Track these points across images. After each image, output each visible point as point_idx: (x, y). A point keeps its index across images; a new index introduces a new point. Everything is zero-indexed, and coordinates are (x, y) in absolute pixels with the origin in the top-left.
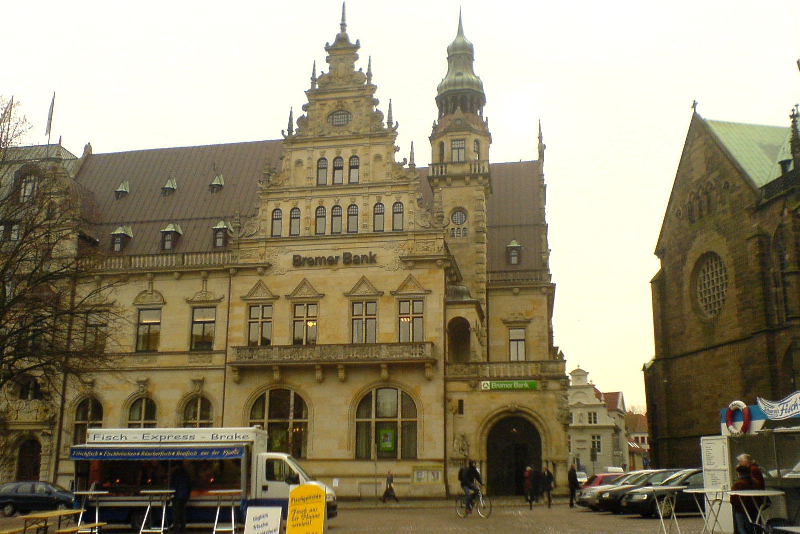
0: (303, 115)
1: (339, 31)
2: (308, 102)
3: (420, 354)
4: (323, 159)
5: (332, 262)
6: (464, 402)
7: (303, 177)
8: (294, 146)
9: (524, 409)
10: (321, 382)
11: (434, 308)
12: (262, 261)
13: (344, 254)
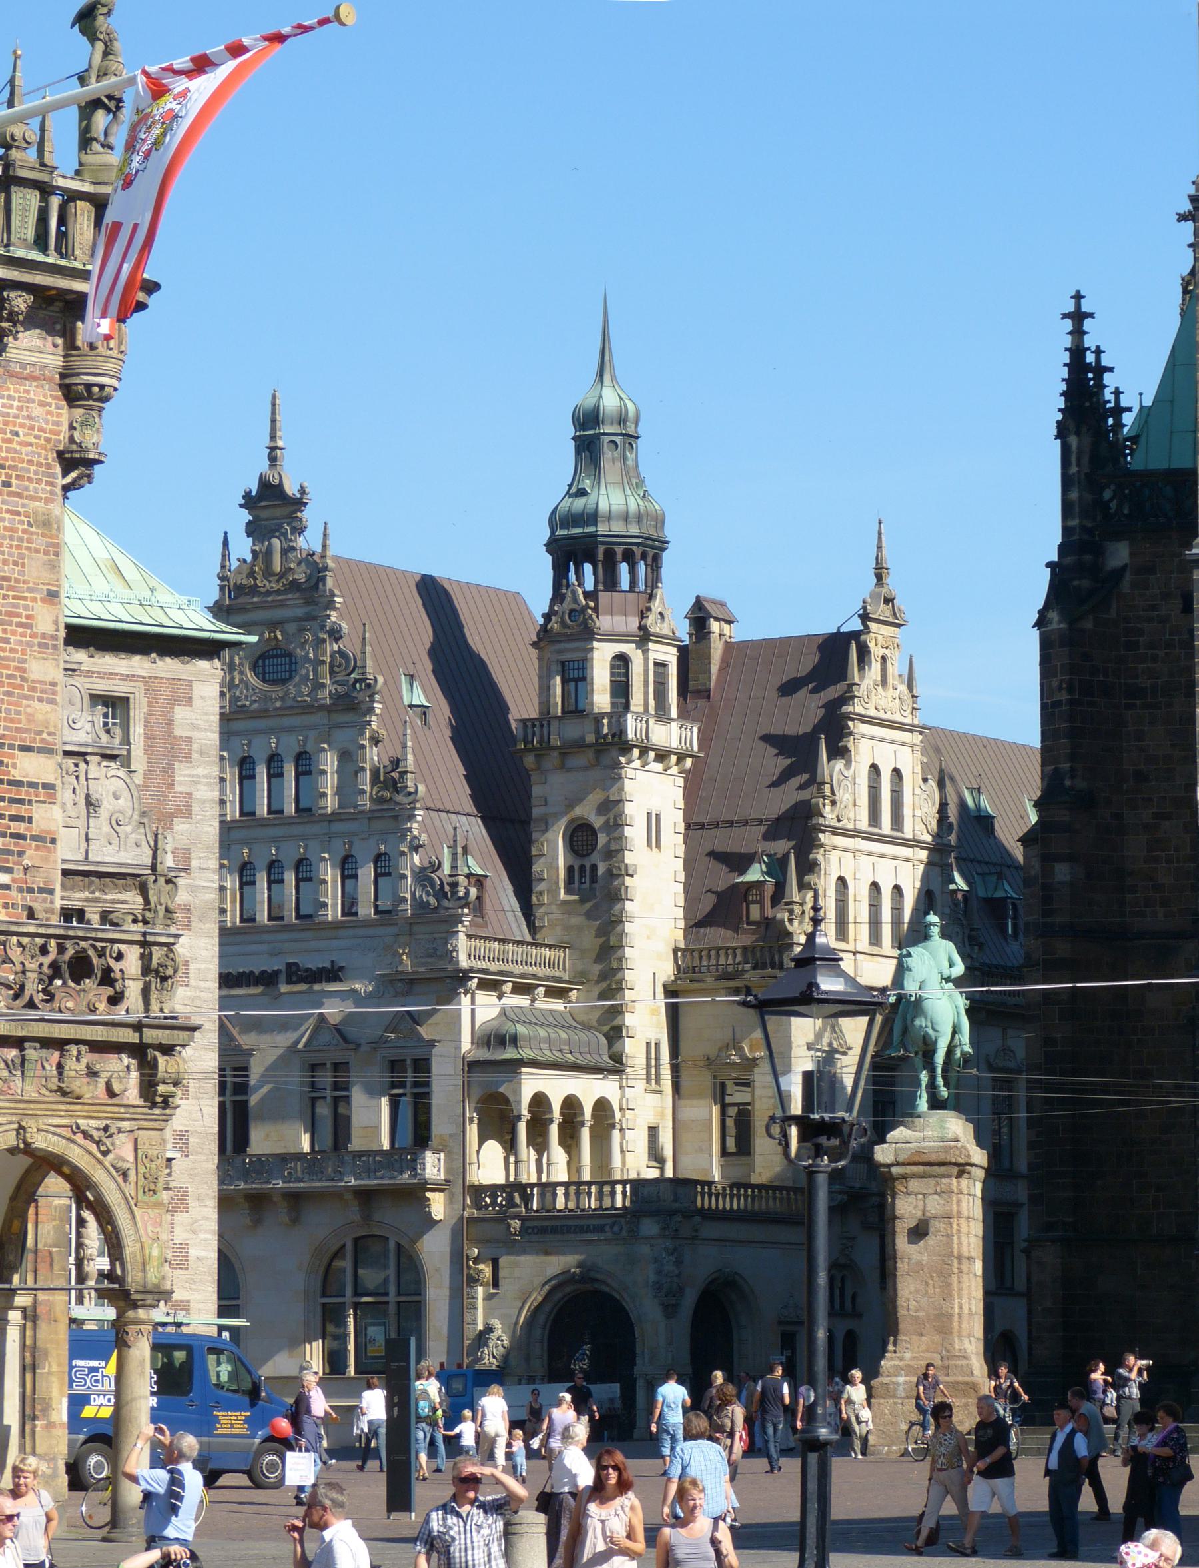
1: (264, 465)
9: (599, 1276)
10: (257, 1222)
13: (289, 965)
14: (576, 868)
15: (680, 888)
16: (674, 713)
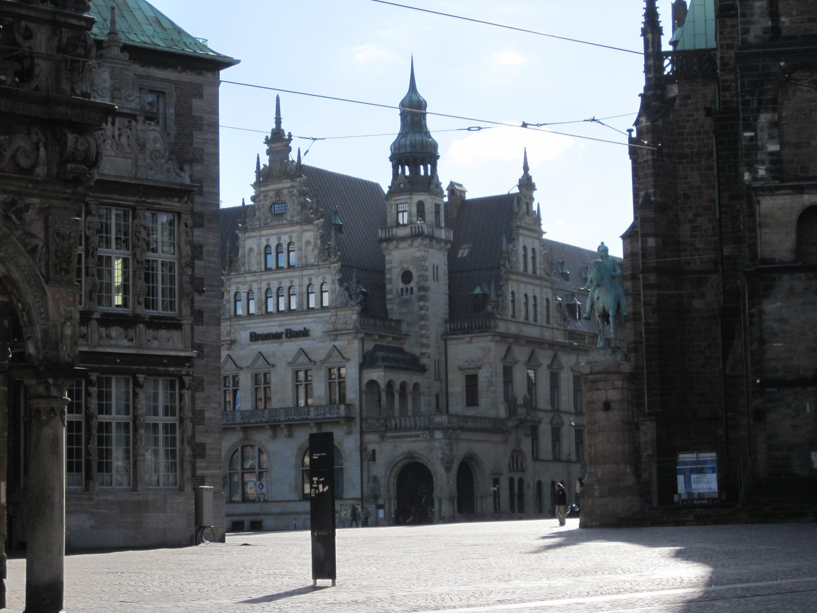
2: (254, 194)
3: (337, 414)
4: (267, 247)
5: (277, 336)
6: (377, 451)
7: (254, 262)
8: (247, 235)
9: (418, 456)
10: (274, 437)
11: (351, 372)
12: (228, 338)
13: (286, 330)
14: (404, 289)
15: (447, 297)
16: (443, 225)
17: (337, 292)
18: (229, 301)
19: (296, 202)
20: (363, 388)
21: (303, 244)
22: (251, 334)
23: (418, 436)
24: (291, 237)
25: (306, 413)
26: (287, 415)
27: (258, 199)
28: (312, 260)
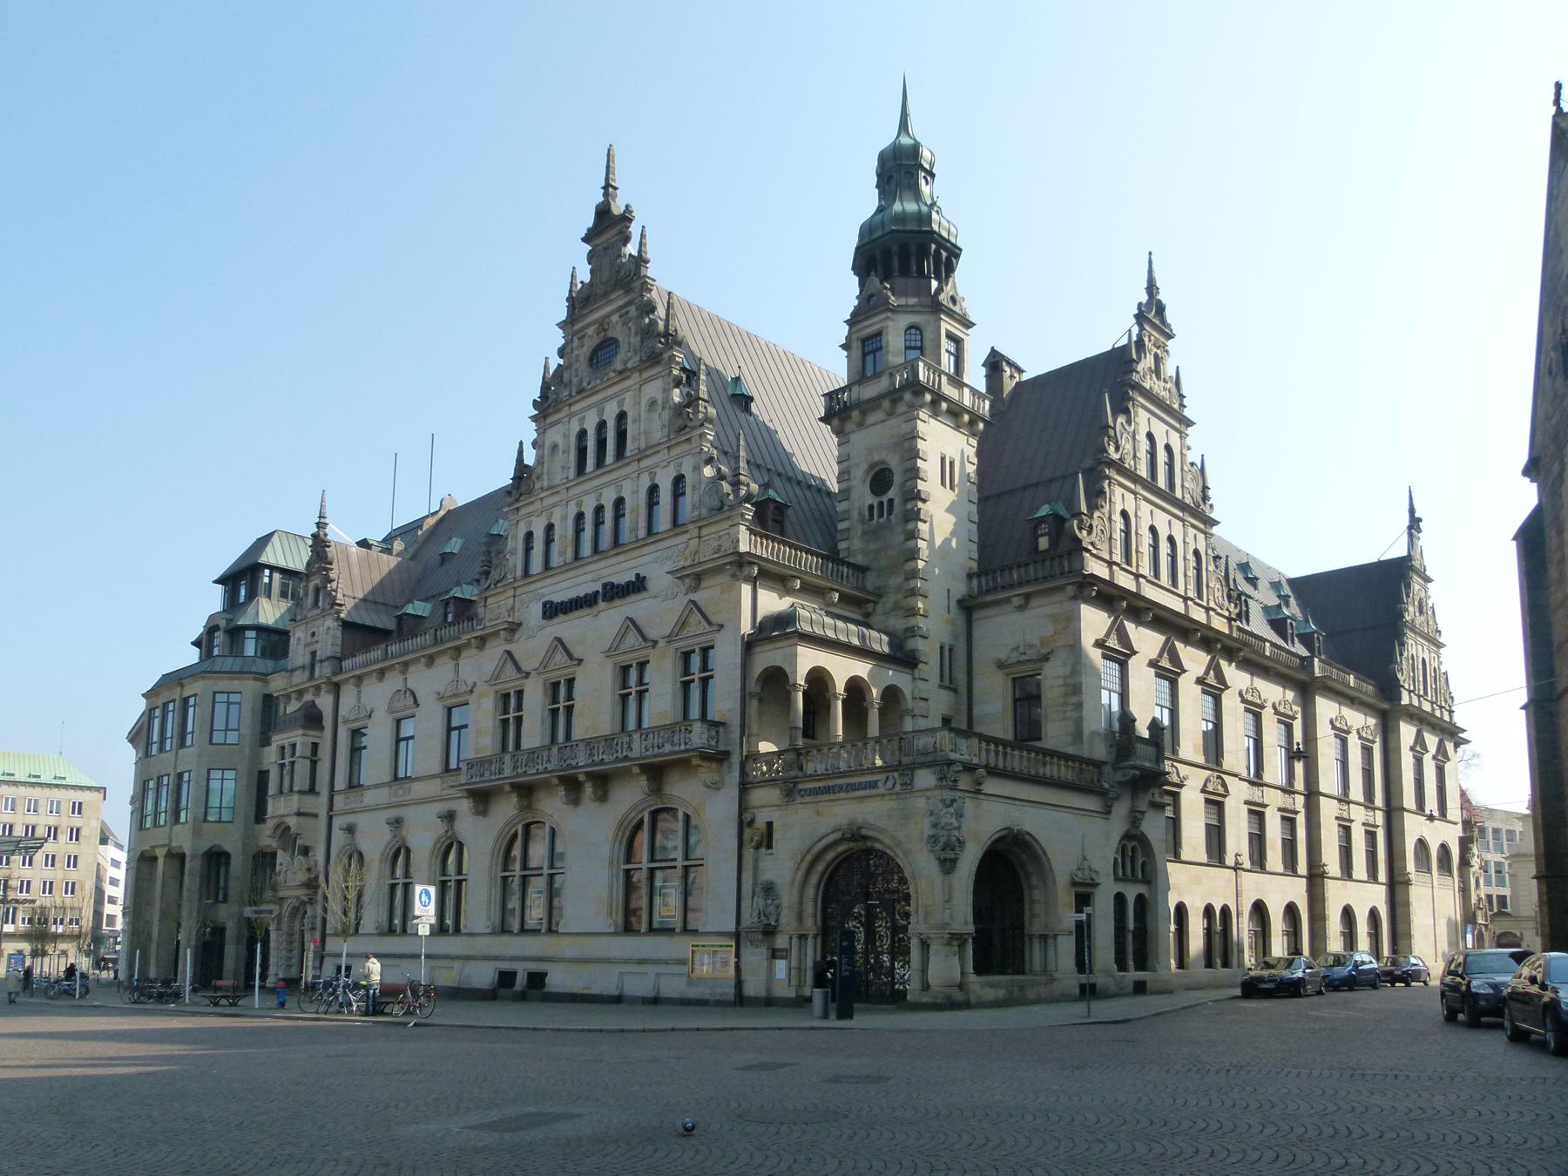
0: (559, 365)
5: (588, 601)
9: (870, 833)
17: (702, 488)
18: (513, 552)
19: (633, 331)
20: (753, 686)
21: (643, 408)
22: (545, 604)
23: (873, 785)
24: (621, 403)
25: (625, 746)
26: (591, 755)
27: (568, 350)
28: (658, 435)
